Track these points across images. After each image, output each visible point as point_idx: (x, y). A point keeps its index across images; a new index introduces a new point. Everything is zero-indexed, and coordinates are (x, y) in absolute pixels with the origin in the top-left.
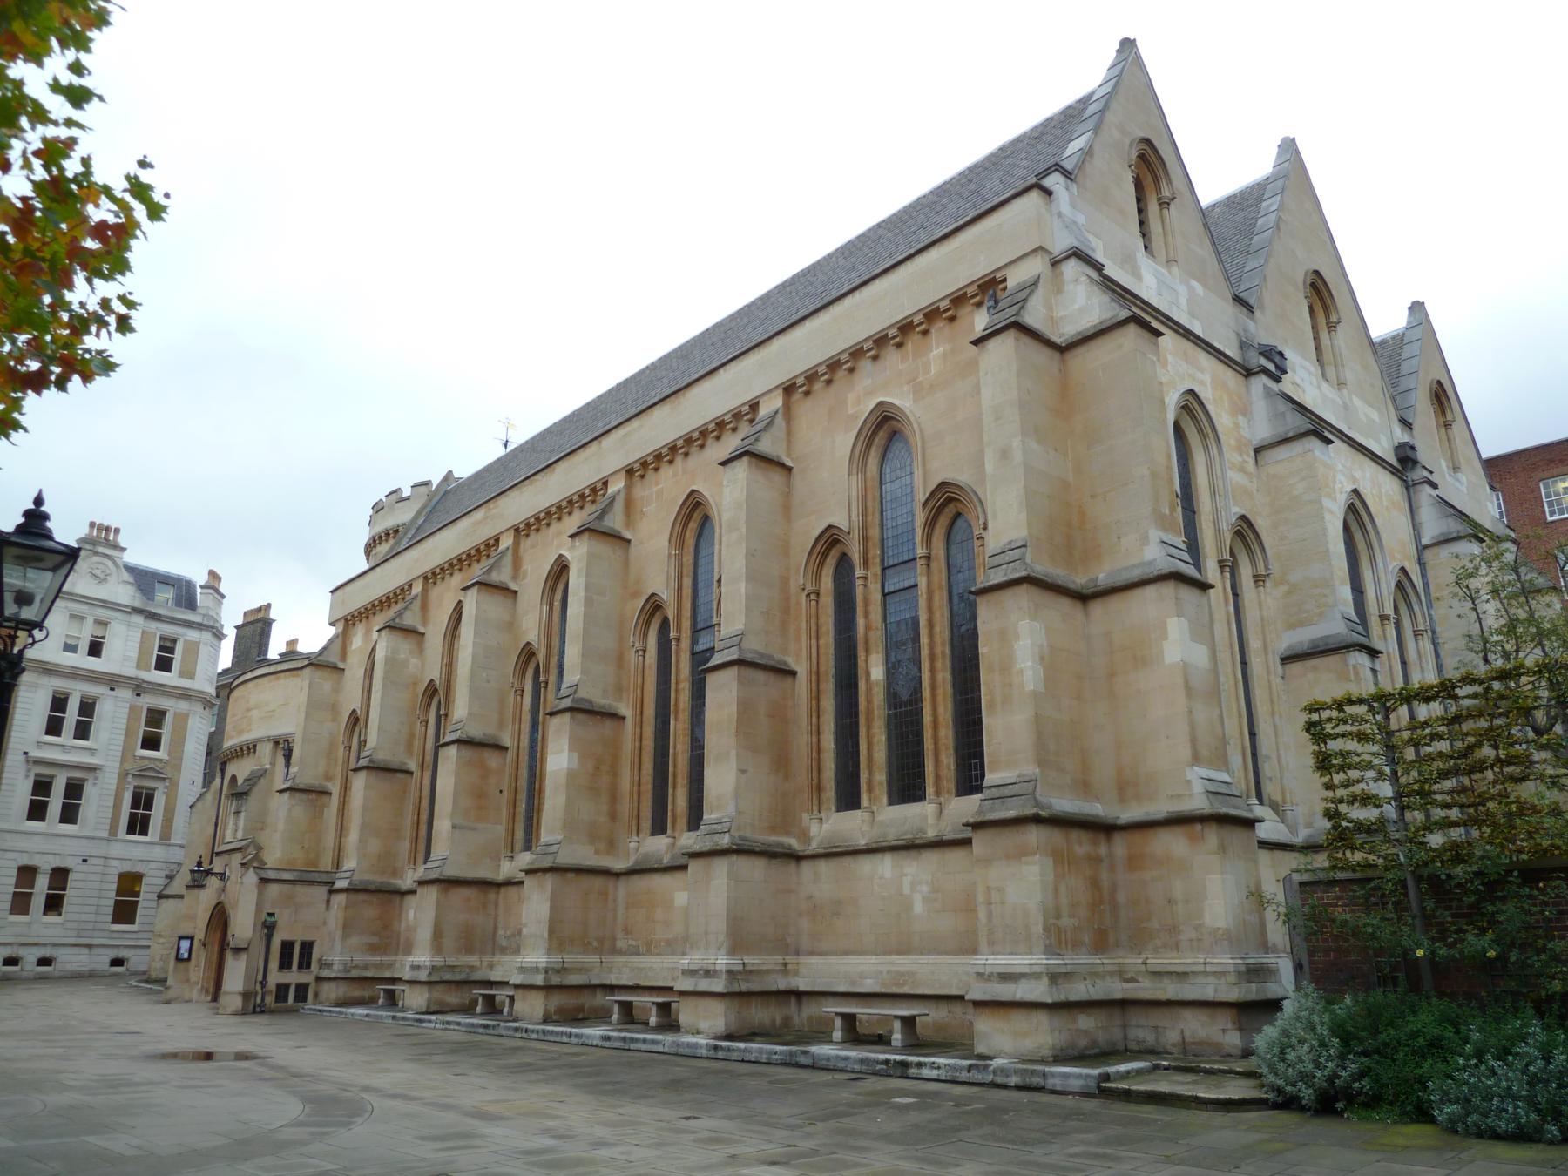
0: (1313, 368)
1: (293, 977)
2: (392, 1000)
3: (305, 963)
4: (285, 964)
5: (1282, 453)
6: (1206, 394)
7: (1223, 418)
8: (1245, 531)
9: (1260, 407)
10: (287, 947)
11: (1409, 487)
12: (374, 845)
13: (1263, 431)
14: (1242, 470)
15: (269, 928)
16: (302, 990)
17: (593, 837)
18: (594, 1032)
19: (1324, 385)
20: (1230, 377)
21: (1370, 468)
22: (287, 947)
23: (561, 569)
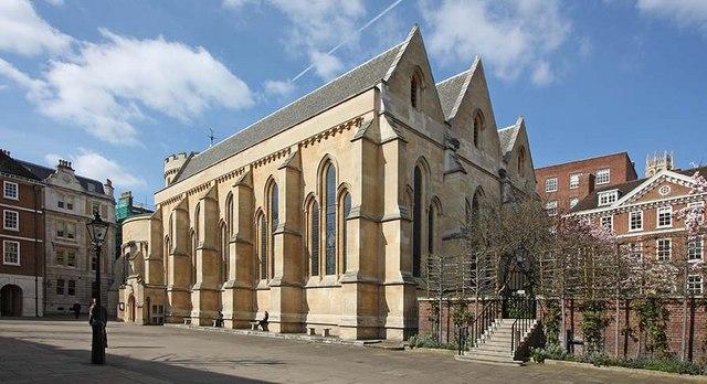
0: (471, 144)
1: (158, 316)
2: (189, 322)
3: (161, 312)
4: (155, 311)
5: (451, 176)
6: (428, 157)
7: (433, 165)
8: (436, 200)
9: (447, 160)
10: (155, 307)
11: (501, 184)
12: (179, 278)
13: (447, 168)
14: (438, 181)
15: (148, 300)
16: (161, 319)
17: (244, 279)
18: (246, 332)
19: (475, 151)
20: (439, 150)
21: (487, 178)
22: (155, 307)
23: (230, 197)
